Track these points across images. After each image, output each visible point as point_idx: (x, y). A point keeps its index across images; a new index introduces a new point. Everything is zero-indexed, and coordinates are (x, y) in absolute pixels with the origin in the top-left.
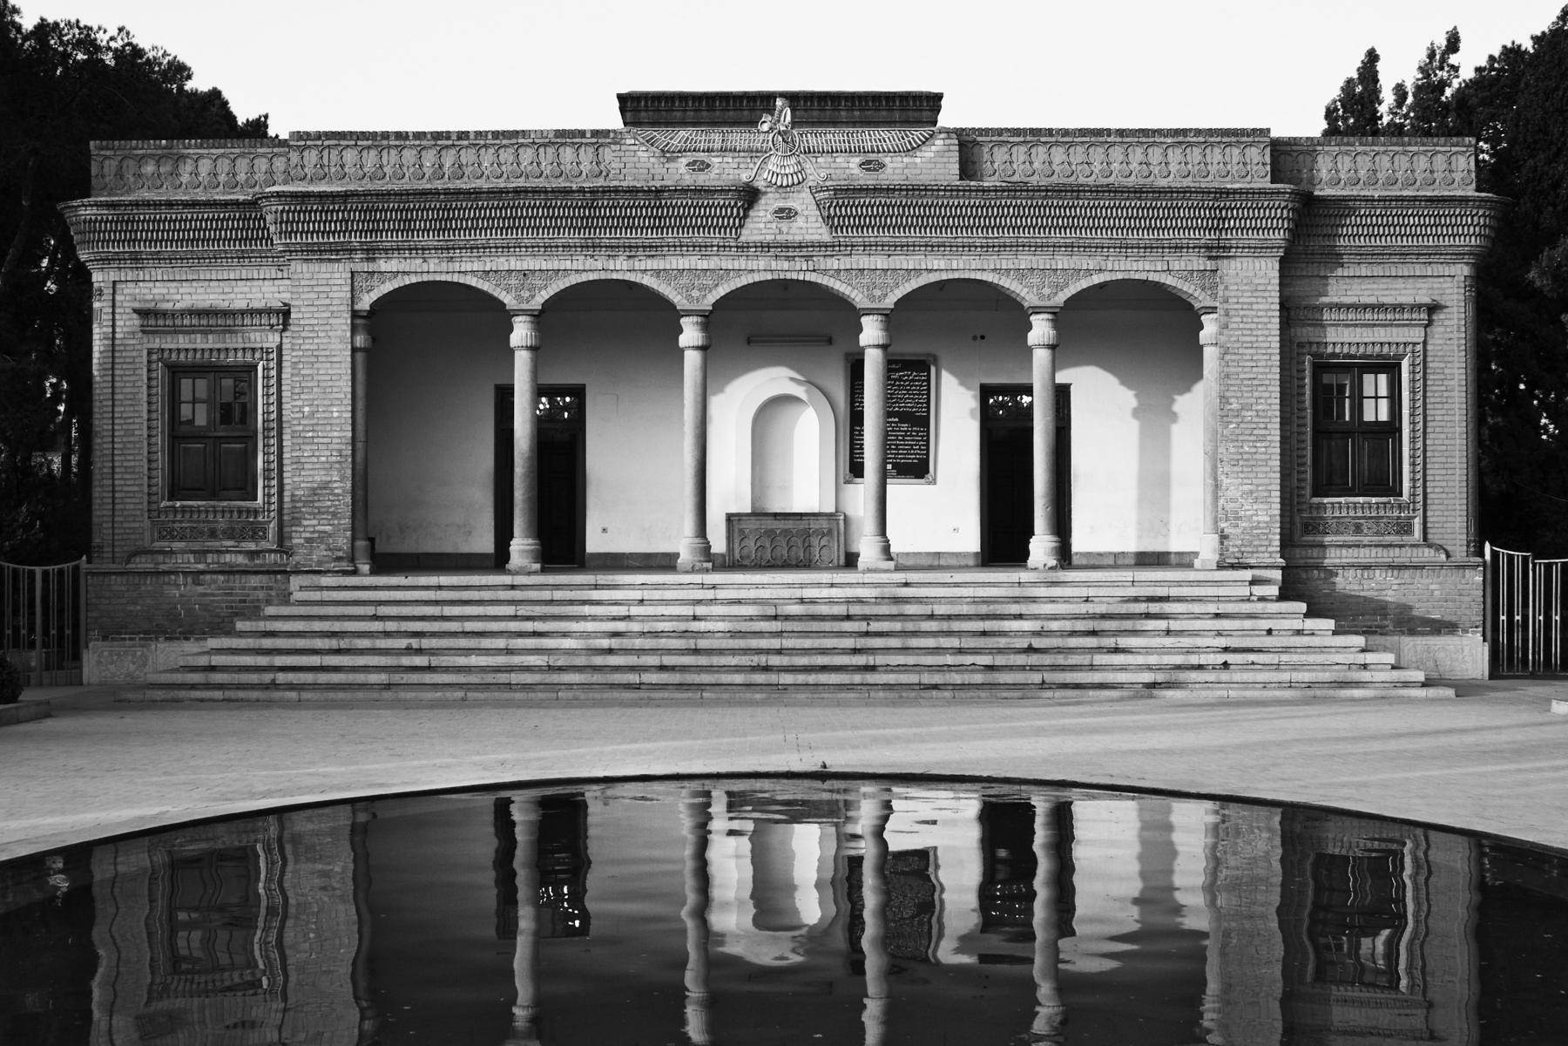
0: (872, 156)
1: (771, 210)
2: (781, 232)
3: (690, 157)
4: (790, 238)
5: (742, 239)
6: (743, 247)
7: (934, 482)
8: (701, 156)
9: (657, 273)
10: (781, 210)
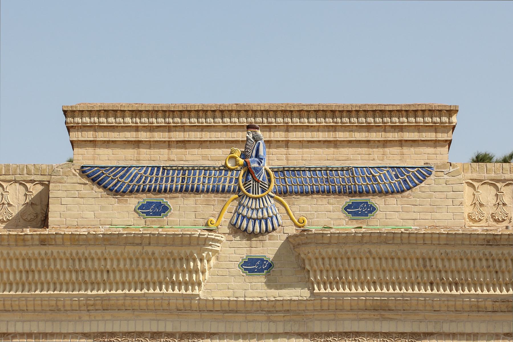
3: (144, 198)
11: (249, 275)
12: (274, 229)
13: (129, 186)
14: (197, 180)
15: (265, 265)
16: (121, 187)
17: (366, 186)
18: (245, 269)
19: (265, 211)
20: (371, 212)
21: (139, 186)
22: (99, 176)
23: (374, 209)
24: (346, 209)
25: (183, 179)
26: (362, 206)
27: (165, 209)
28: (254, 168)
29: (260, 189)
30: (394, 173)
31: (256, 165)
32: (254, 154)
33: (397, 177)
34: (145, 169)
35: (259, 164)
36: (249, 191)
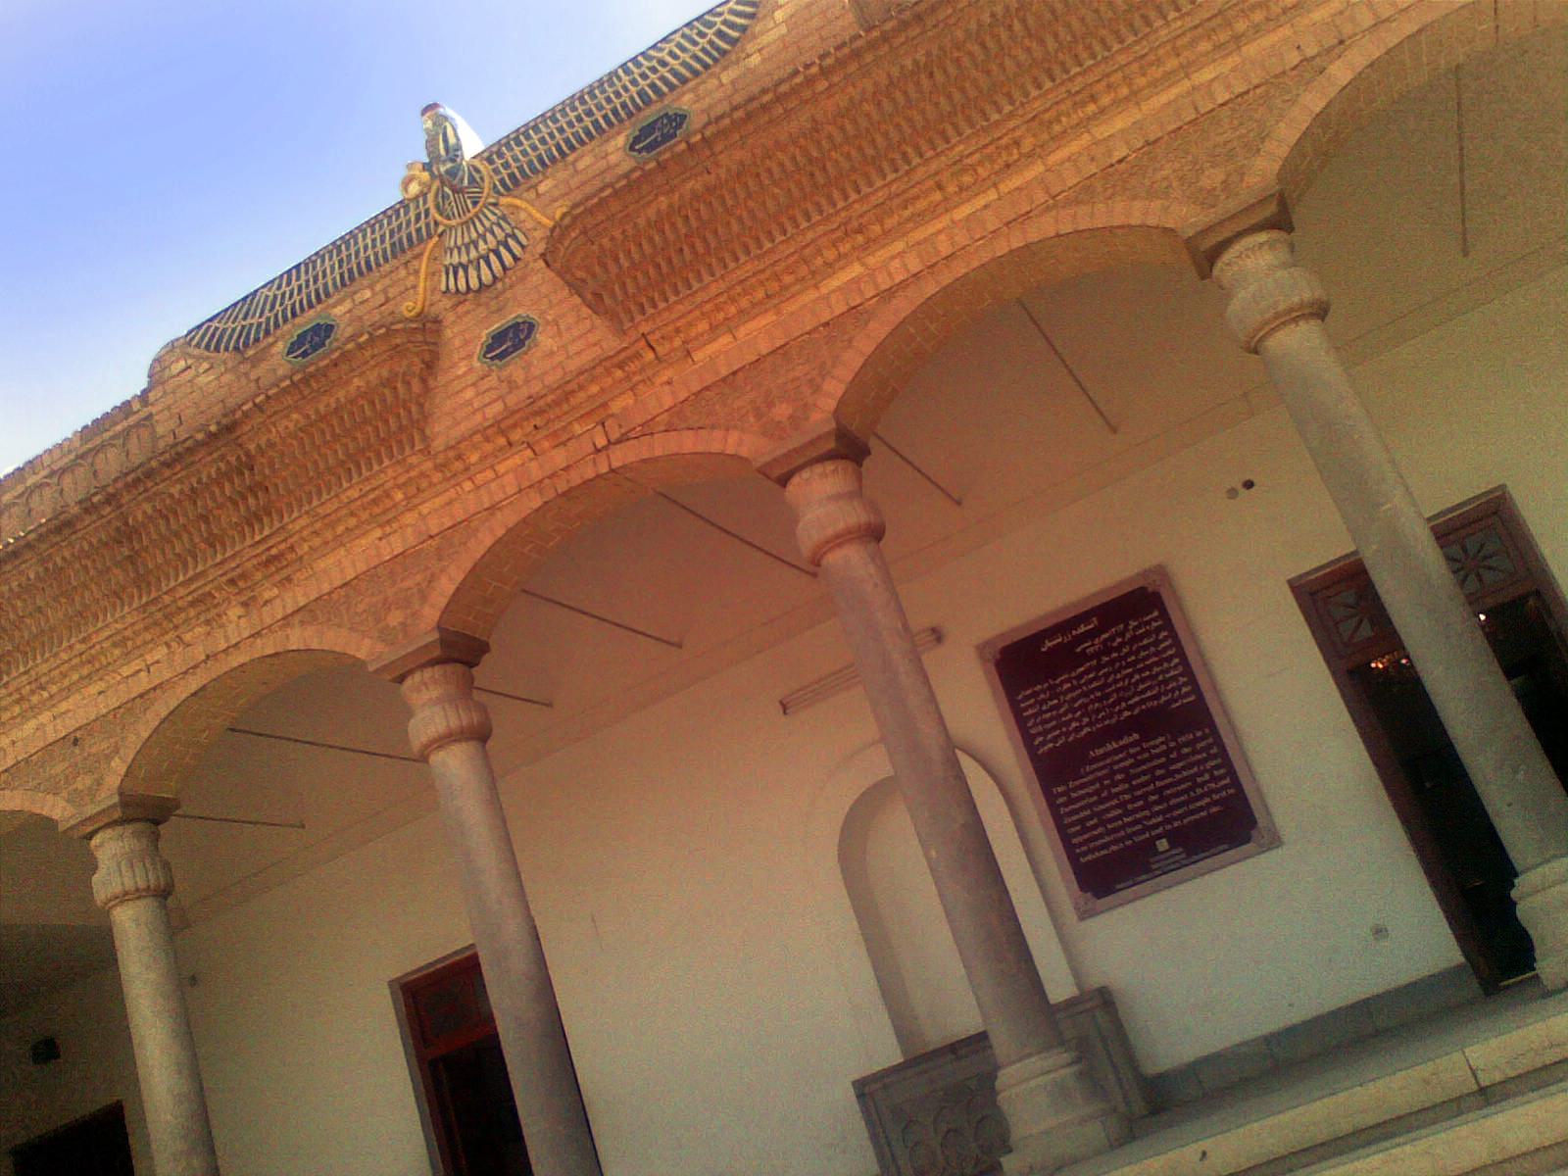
0: (649, 114)
1: (478, 350)
2: (512, 386)
4: (536, 388)
5: (438, 444)
6: (453, 464)
7: (1275, 841)
8: (308, 319)
9: (306, 613)
10: (498, 338)
11: (505, 365)
12: (516, 258)
13: (259, 325)
14: (362, 250)
15: (522, 330)
16: (248, 334)
17: (653, 86)
18: (492, 358)
19: (489, 236)
20: (680, 126)
21: (276, 316)
22: (213, 335)
23: (684, 117)
24: (632, 148)
25: (341, 262)
26: (659, 125)
27: (330, 328)
28: (447, 172)
29: (469, 202)
30: (695, 31)
31: (449, 165)
32: (442, 152)
33: (702, 35)
34: (277, 282)
35: (453, 160)
36: (448, 218)
